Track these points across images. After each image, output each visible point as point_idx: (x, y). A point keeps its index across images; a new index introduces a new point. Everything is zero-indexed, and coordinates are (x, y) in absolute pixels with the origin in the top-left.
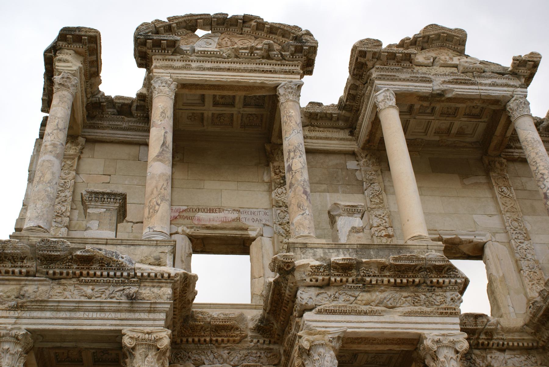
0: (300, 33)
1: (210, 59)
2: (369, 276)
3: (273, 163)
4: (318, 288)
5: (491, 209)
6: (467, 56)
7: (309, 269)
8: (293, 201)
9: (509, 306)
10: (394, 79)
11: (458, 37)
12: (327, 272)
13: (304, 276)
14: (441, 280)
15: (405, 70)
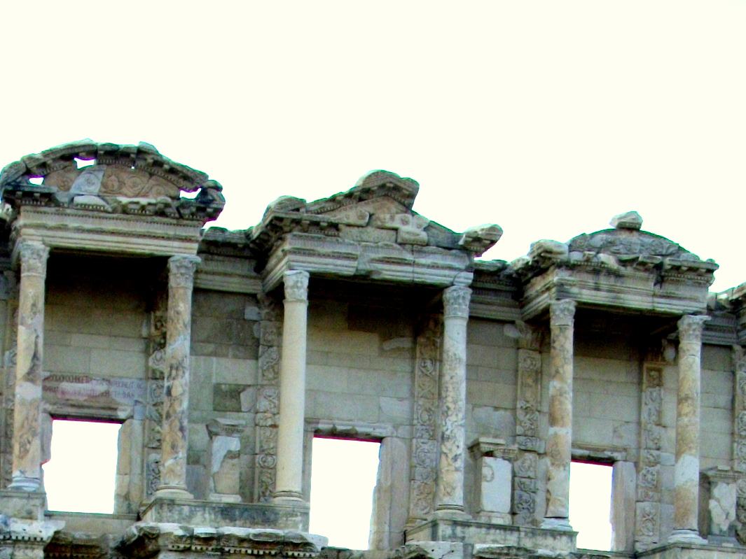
0: (205, 185)
1: (90, 213)
2: (228, 546)
3: (155, 312)
4: (178, 553)
5: (404, 391)
6: (414, 214)
7: (172, 537)
8: (168, 438)
9: (385, 523)
10: (311, 253)
11: (407, 190)
12: (189, 541)
13: (166, 542)
14: (296, 554)
15: (328, 239)
